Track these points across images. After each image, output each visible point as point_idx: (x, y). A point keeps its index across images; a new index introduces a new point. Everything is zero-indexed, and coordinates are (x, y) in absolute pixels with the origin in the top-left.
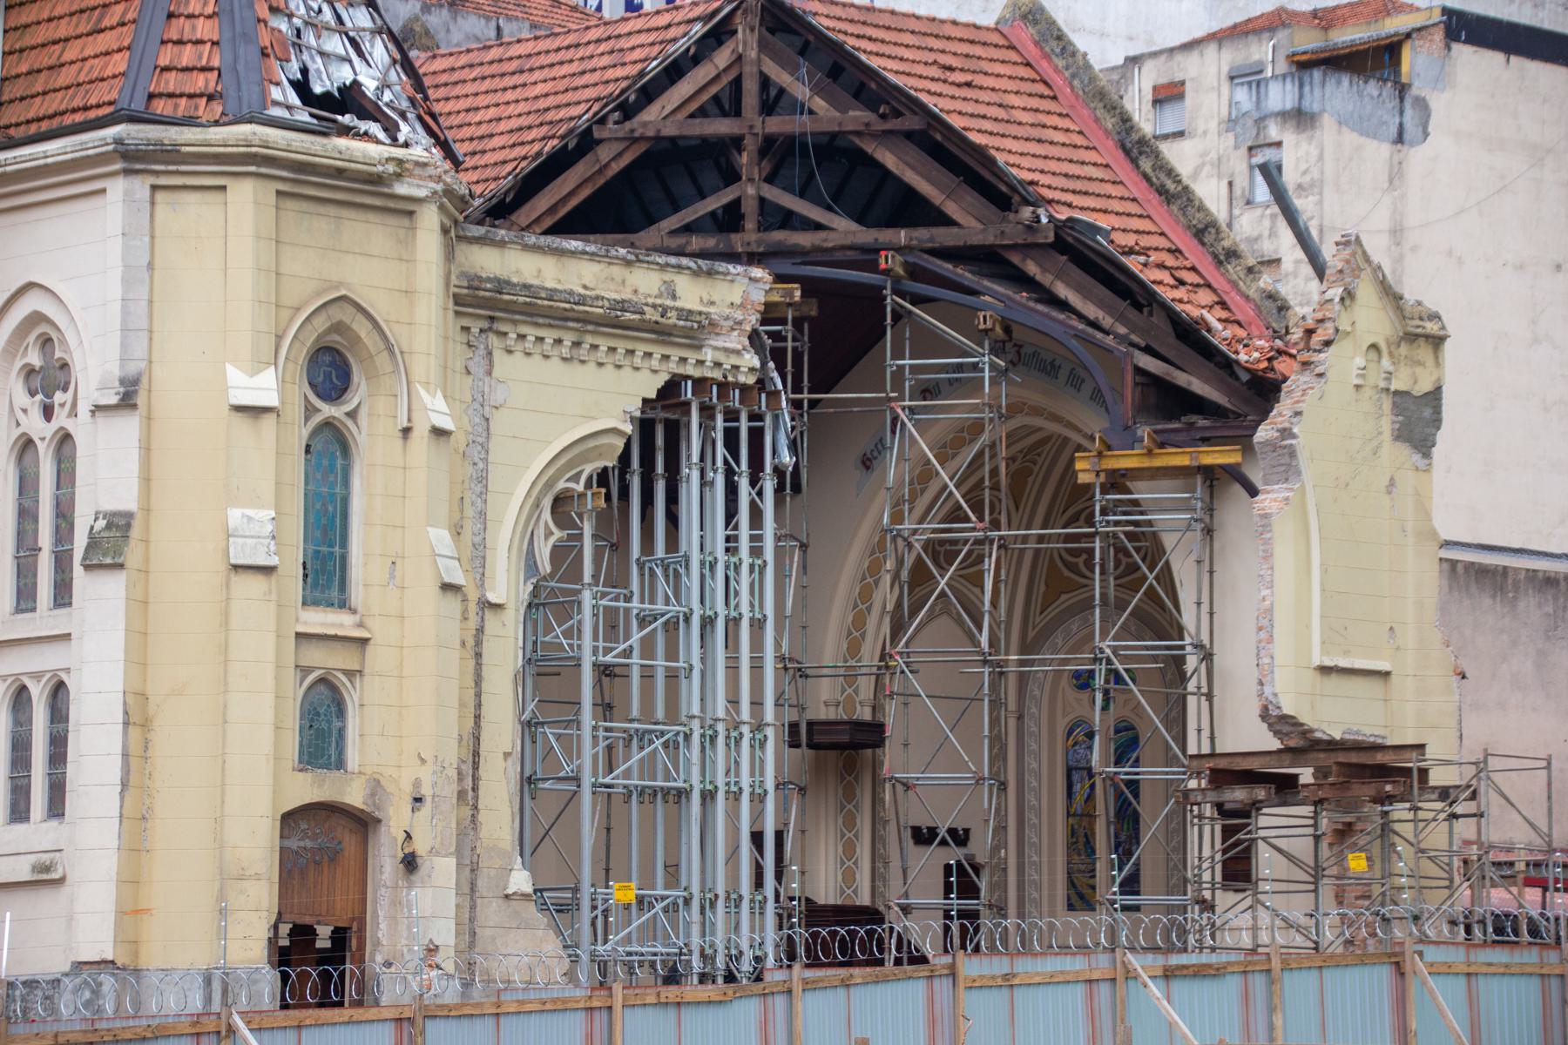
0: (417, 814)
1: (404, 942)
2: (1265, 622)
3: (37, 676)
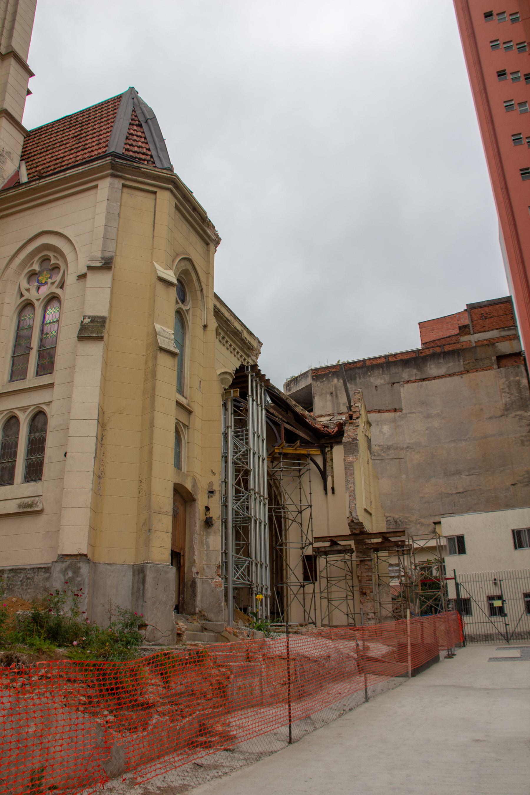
0: (211, 499)
1: (204, 562)
2: (352, 494)
3: (23, 409)
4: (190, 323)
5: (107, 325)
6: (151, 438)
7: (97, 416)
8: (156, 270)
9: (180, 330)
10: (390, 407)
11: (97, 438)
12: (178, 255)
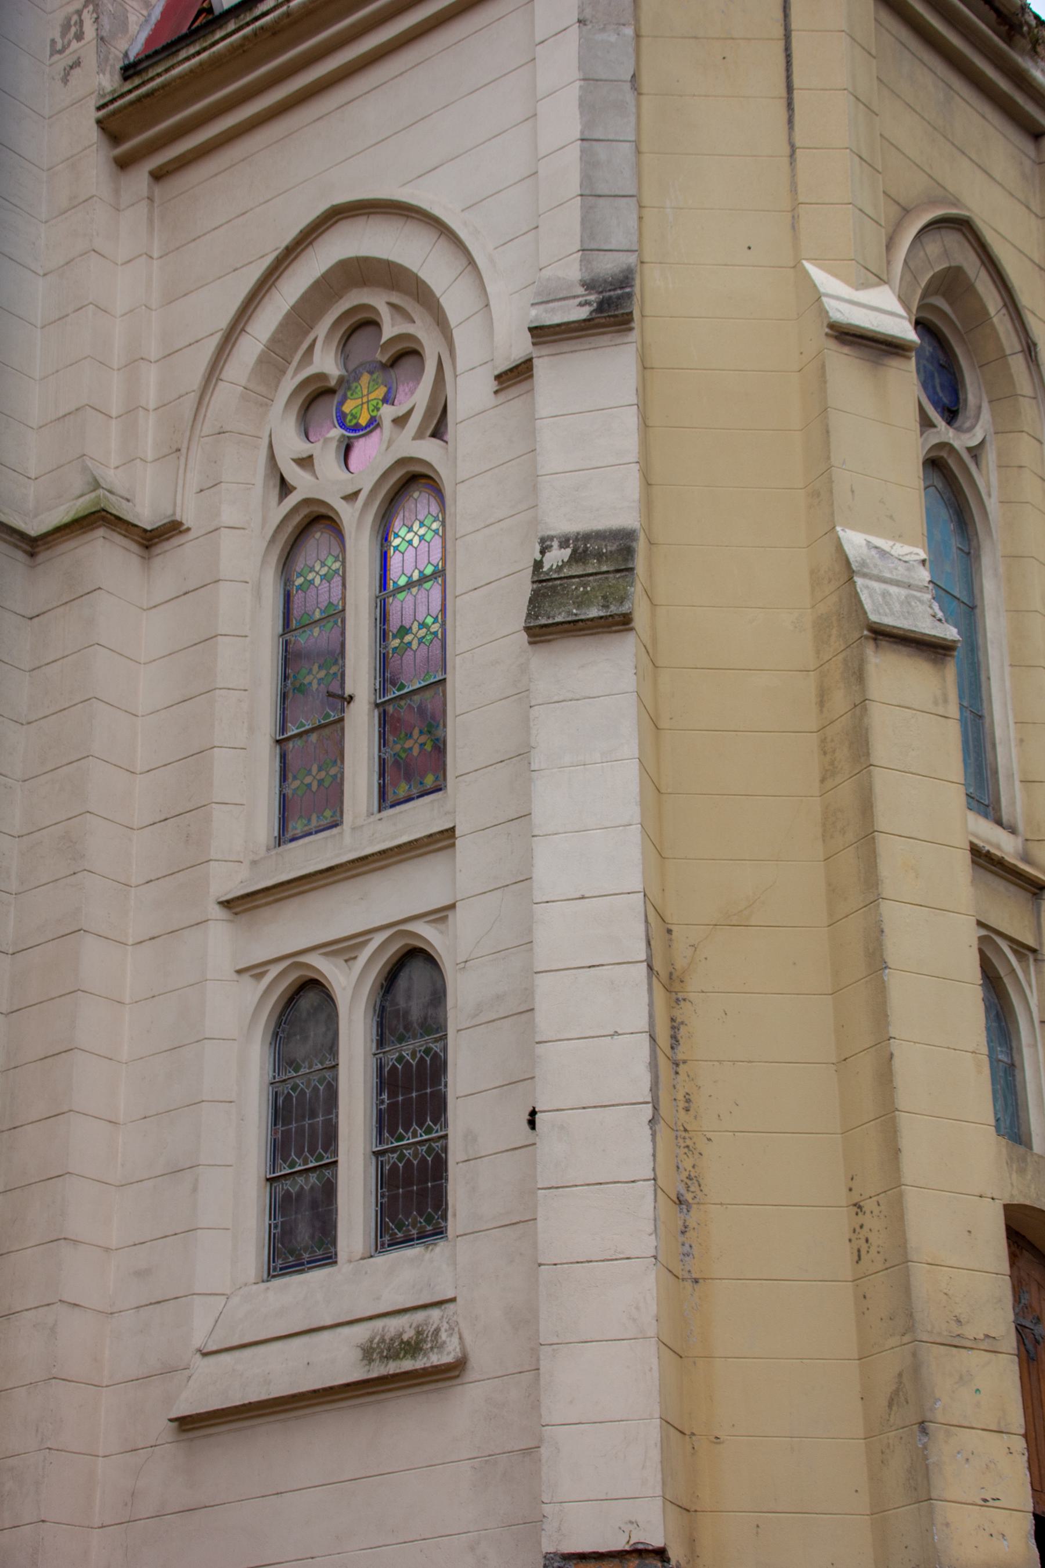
4: (992, 504)
5: (640, 563)
6: (880, 1014)
7: (642, 945)
8: (818, 297)
9: (955, 542)
11: (653, 1038)
12: (906, 212)
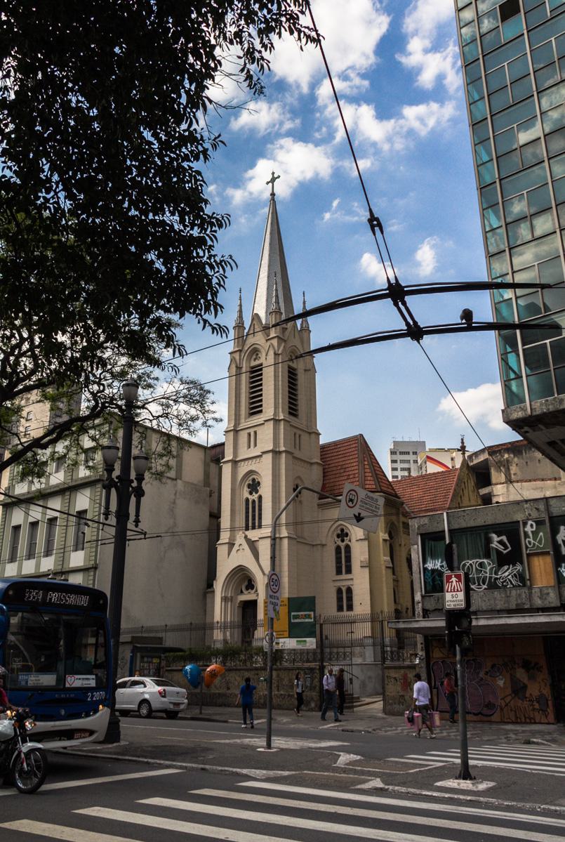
3: (344, 586)
10: (551, 476)
